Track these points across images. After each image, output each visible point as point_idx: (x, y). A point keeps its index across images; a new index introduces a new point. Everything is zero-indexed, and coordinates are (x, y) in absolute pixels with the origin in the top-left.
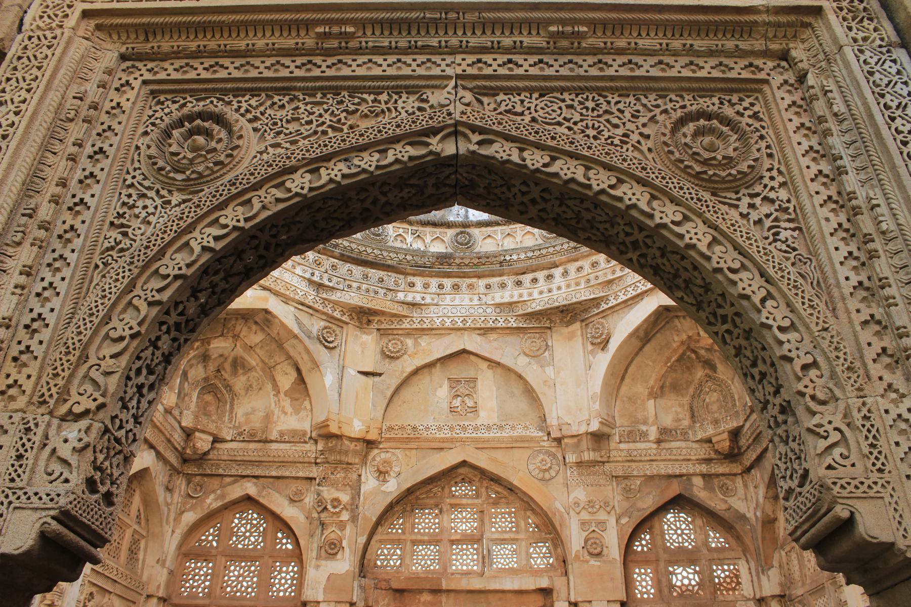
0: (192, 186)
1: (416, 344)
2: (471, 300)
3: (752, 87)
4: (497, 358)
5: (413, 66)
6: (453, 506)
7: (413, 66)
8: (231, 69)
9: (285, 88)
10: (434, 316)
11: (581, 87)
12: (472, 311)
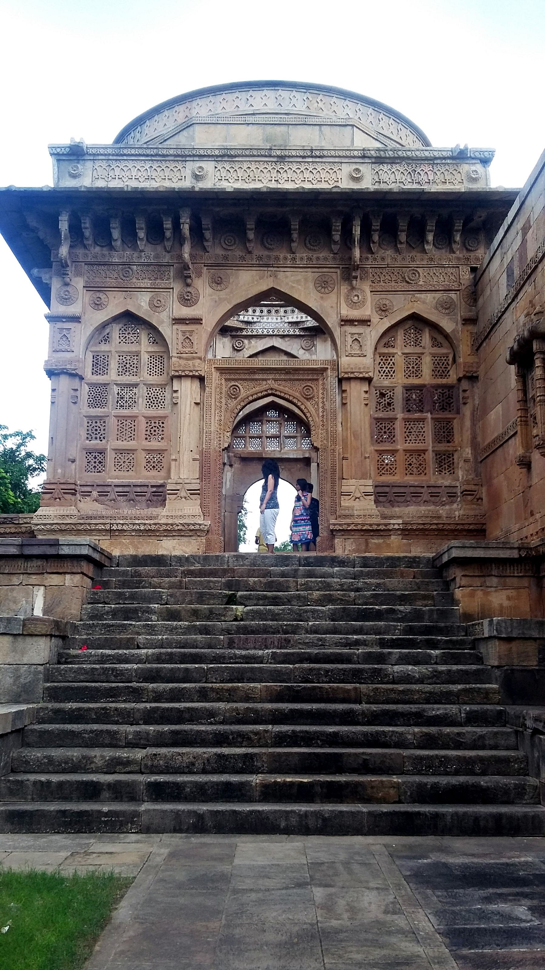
0: (236, 398)
1: (250, 343)
2: (277, 319)
3: (317, 380)
4: (289, 350)
5: (265, 377)
6: (269, 421)
7: (265, 377)
8: (237, 377)
9: (246, 380)
10: (258, 329)
11: (290, 380)
12: (277, 325)
